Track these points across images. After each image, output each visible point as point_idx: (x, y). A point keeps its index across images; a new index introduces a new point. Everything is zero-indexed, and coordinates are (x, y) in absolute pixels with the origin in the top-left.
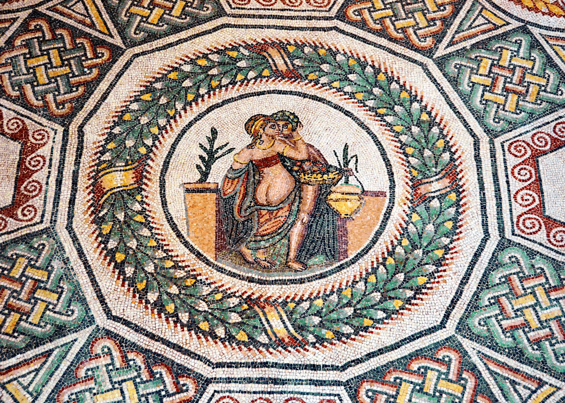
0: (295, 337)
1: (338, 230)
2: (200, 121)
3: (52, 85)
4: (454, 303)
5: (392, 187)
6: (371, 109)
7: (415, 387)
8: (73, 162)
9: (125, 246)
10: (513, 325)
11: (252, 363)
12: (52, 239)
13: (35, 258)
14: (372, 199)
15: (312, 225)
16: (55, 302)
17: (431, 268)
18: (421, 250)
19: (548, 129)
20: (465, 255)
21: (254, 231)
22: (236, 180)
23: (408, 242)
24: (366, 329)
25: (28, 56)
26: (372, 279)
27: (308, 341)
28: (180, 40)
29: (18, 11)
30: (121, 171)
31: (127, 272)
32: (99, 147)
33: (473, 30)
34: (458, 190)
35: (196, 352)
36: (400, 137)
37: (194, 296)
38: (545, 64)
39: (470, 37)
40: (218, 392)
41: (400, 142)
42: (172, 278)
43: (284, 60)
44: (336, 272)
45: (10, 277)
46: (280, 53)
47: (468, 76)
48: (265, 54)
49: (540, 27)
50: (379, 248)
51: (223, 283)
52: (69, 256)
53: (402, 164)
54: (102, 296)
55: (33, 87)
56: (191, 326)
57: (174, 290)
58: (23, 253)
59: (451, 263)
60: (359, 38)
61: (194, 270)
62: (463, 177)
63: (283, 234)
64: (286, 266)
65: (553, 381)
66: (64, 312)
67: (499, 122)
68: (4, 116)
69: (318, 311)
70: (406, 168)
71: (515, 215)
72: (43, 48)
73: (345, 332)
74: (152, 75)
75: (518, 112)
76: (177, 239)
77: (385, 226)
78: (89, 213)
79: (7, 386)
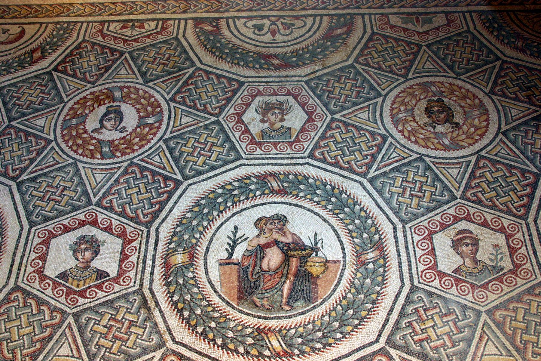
3: (141, 204)
4: (384, 326)
5: (344, 257)
6: (330, 210)
9: (184, 299)
12: (140, 296)
14: (332, 265)
16: (142, 334)
17: (369, 306)
19: (438, 218)
21: (261, 287)
23: (355, 291)
24: (330, 345)
26: (333, 314)
29: (122, 162)
34: (384, 257)
38: (434, 179)
41: (348, 229)
47: (388, 188)
48: (266, 180)
49: (430, 157)
50: (337, 295)
54: (170, 330)
55: (130, 206)
57: (213, 325)
59: (382, 302)
60: (322, 169)
61: (225, 312)
63: (278, 289)
64: (281, 308)
71: (420, 270)
78: (162, 279)
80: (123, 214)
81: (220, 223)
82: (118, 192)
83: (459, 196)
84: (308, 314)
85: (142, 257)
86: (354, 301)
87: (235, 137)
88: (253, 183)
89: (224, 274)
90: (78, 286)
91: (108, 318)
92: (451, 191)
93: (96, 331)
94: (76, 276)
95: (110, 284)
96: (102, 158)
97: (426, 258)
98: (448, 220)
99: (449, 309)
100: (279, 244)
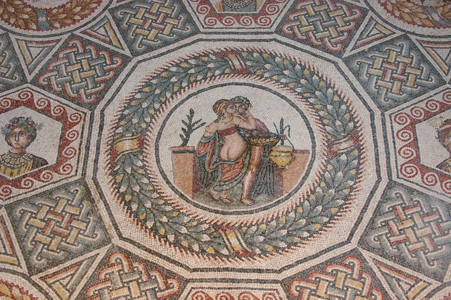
0: (247, 251)
1: (277, 177)
2: (183, 105)
3: (83, 83)
4: (356, 225)
5: (314, 147)
6: (299, 94)
7: (329, 284)
8: (97, 135)
9: (132, 190)
10: (398, 240)
11: (218, 268)
12: (82, 187)
13: (71, 199)
14: (300, 155)
15: (258, 174)
16: (85, 229)
17: (341, 202)
18: (334, 190)
19: (423, 105)
20: (364, 192)
21: (219, 179)
22: (207, 144)
23: (325, 184)
24: (295, 244)
25: (68, 64)
26: (300, 210)
27: (256, 253)
28: (169, 51)
29: (61, 34)
30: (129, 139)
31: (133, 208)
32: (115, 124)
33: (370, 38)
34: (360, 148)
35: (179, 261)
36: (319, 112)
37: (178, 223)
38: (420, 60)
39: (368, 43)
40: (194, 288)
41: (319, 116)
42: (163, 211)
43: (240, 62)
44: (275, 206)
45: (55, 212)
46: (237, 58)
47: (366, 70)
48: (227, 58)
49: (417, 35)
50: (305, 189)
51: (198, 214)
52: (94, 197)
53: (321, 131)
54: (116, 224)
55: (71, 84)
56: (176, 244)
58: (63, 196)
61: (178, 206)
62: (363, 139)
63: (238, 181)
65: (426, 278)
66: (91, 236)
67: (388, 101)
68: (52, 105)
69: (262, 233)
70: (323, 134)
71: (399, 164)
72: (78, 59)
73: (281, 247)
74: (150, 74)
75: (401, 93)
76: (167, 185)
77: (309, 173)
78: (108, 168)
79: (52, 285)
80: (63, 94)
81: (174, 106)
82: (57, 69)
83: (448, 81)
84: (272, 210)
85: (84, 142)
86: (324, 196)
87: (192, 8)
88: (211, 61)
89: (178, 162)
90: (11, 174)
91: (46, 211)
92: (439, 75)
93: (33, 226)
94: (9, 163)
95: (48, 173)
96: (38, 30)
97: (407, 150)
98: (434, 108)
99: (432, 209)
100: (240, 131)
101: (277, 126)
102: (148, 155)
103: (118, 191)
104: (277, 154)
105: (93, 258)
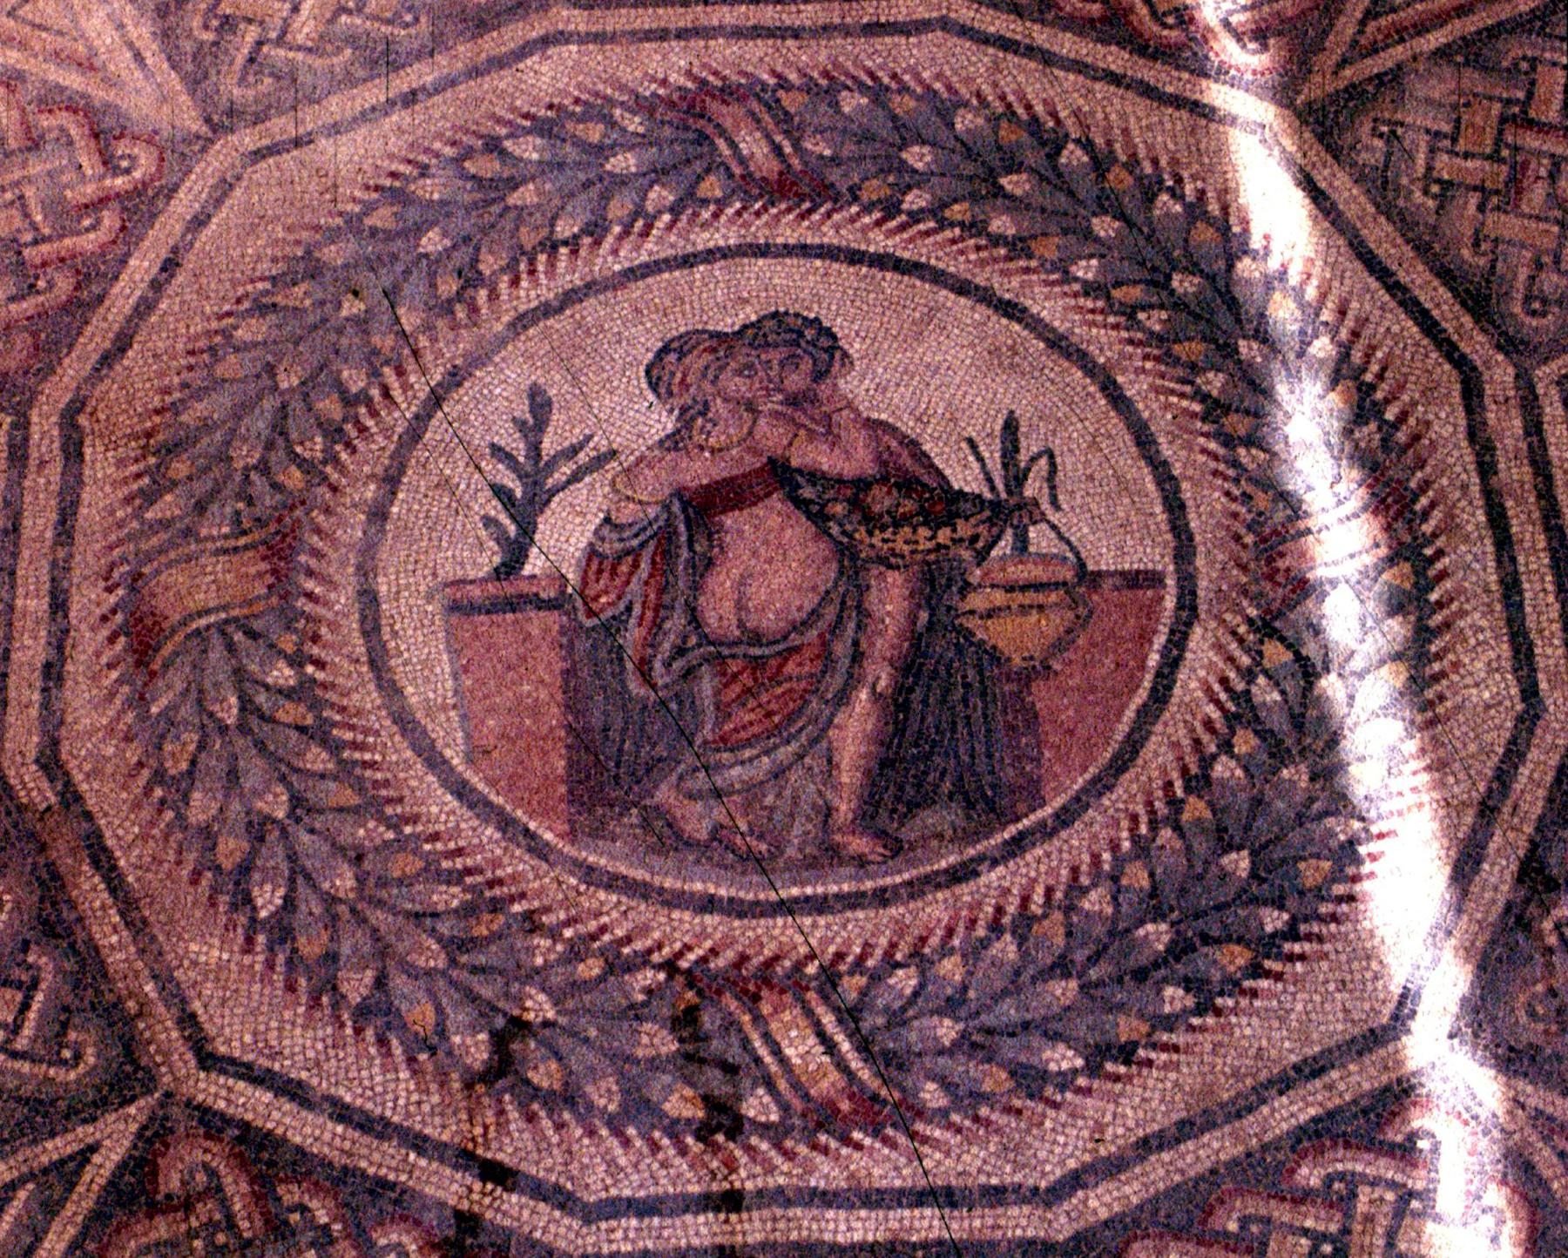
6: (1089, 289)
8: (49, 534)
23: (1254, 741)
24: (1126, 1053)
31: (260, 902)
32: (138, 476)
73: (1053, 1067)
84: (992, 877)
101: (986, 455)
102: (324, 630)
103: (180, 816)
104: (999, 597)
105: (69, 1170)
